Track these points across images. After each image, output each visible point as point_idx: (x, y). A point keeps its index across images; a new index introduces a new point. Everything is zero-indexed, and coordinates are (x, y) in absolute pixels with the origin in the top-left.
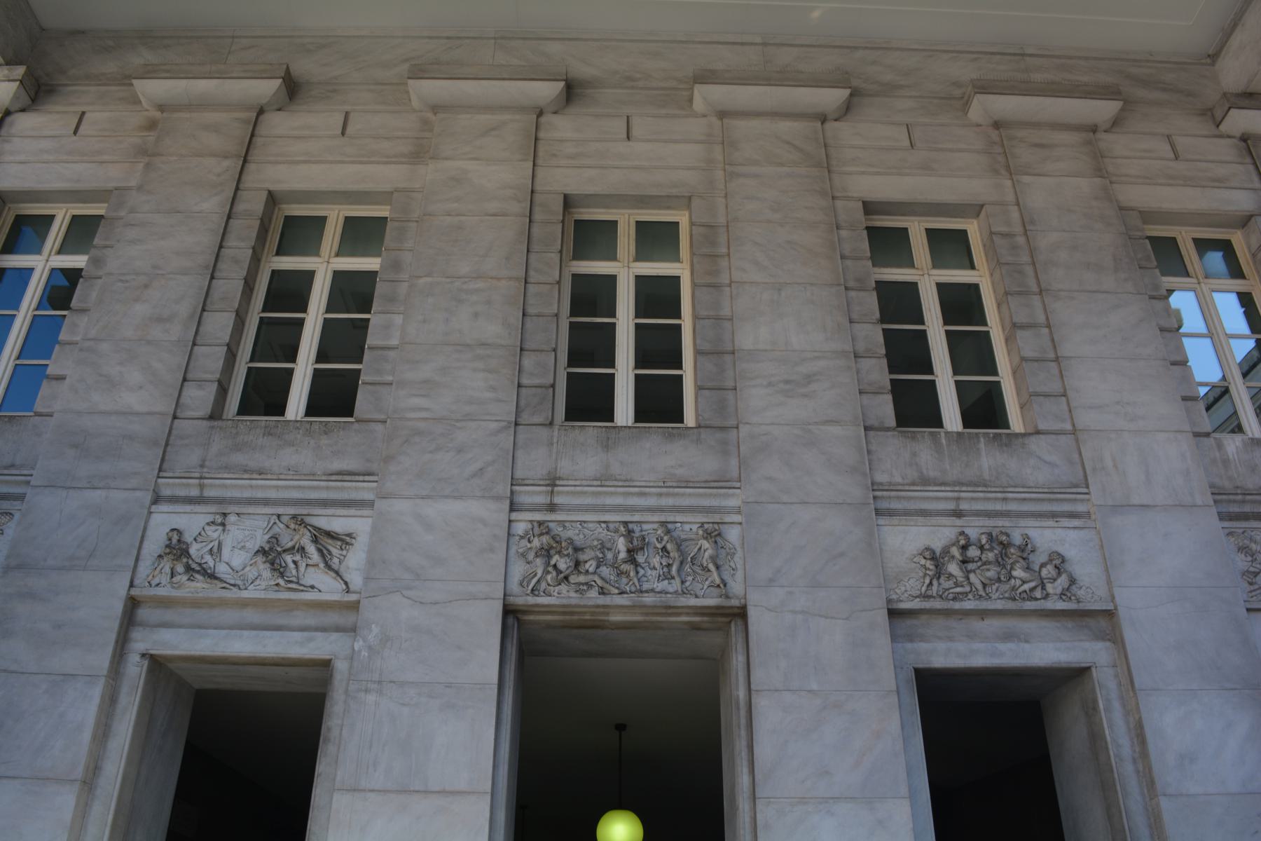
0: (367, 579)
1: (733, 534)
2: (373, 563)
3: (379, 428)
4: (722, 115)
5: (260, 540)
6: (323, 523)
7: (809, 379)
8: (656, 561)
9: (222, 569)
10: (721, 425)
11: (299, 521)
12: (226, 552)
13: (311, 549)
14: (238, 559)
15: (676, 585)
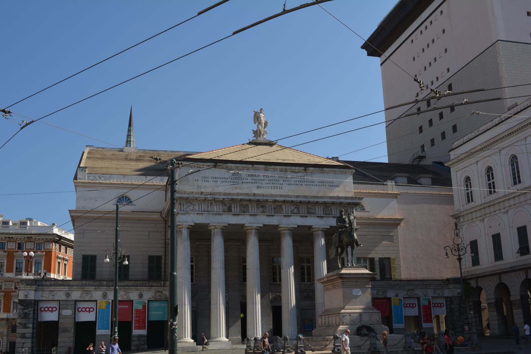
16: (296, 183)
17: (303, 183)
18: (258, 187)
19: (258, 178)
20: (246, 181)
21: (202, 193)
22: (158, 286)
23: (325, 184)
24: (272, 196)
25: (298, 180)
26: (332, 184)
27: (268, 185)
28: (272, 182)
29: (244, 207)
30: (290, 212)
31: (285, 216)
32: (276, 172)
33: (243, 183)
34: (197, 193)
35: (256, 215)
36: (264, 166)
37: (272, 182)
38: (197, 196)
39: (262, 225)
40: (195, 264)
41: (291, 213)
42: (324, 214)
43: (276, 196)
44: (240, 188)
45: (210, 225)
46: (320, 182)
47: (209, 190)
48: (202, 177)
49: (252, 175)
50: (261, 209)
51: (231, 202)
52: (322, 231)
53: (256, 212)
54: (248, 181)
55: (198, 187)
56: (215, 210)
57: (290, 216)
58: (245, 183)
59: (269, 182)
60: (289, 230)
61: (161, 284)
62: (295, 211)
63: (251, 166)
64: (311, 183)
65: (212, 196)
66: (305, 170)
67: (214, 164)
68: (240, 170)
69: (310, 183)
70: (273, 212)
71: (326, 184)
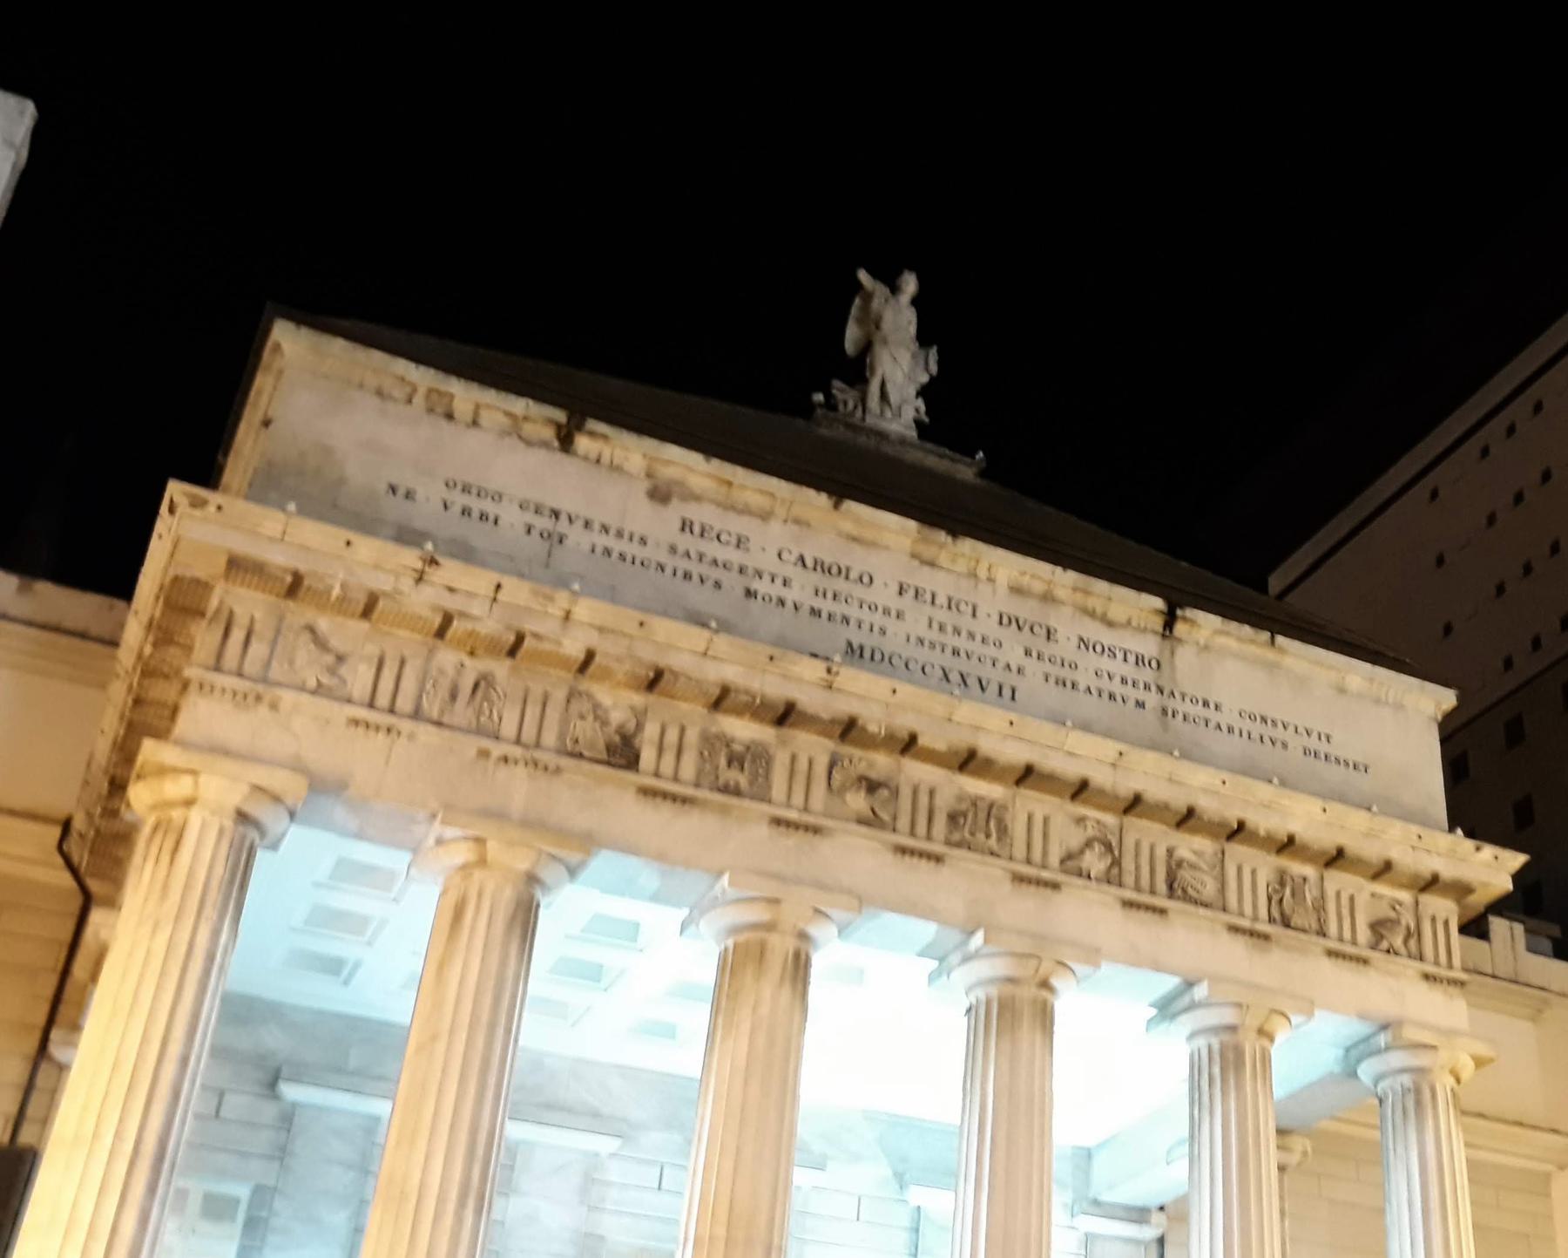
16: (1105, 684)
19: (859, 591)
20: (777, 590)
26: (1323, 748)
27: (923, 655)
29: (735, 760)
32: (985, 588)
33: (750, 594)
37: (951, 641)
49: (819, 565)
50: (858, 801)
51: (638, 699)
54: (790, 595)
56: (509, 728)
58: (767, 599)
59: (934, 635)
64: (1199, 710)
66: (1170, 621)
68: (746, 511)
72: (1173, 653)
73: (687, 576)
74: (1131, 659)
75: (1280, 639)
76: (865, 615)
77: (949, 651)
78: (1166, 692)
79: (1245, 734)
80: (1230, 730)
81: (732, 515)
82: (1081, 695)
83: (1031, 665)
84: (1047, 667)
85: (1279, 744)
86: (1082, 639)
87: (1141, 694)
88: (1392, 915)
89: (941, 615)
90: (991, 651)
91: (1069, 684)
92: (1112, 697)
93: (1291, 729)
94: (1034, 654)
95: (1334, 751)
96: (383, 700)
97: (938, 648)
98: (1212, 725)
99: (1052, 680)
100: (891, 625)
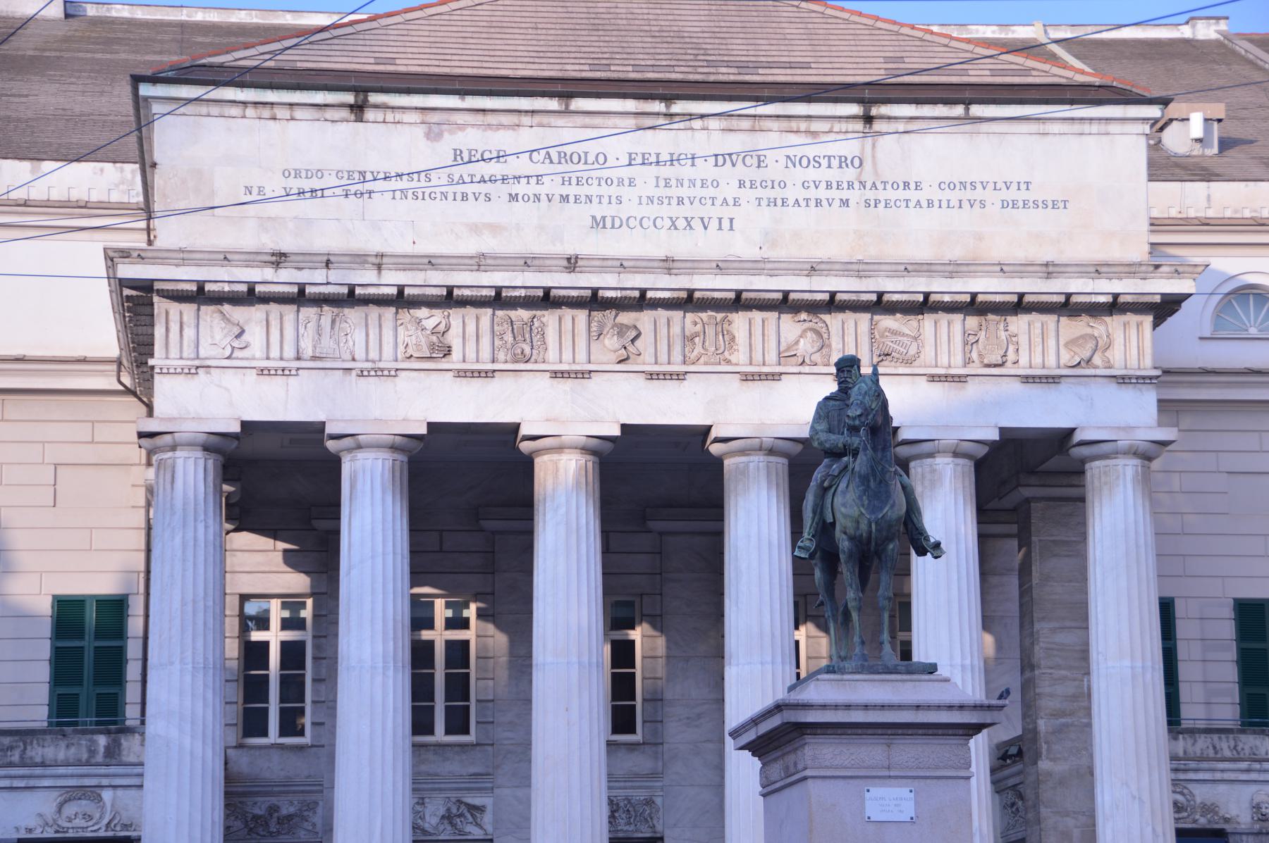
0: (495, 829)
1: (658, 801)
2: (496, 822)
3: (490, 748)
4: (661, 534)
5: (442, 811)
6: (470, 801)
7: (699, 716)
8: (624, 816)
9: (427, 826)
10: (653, 744)
11: (460, 802)
12: (427, 817)
13: (469, 816)
14: (434, 821)
15: (632, 828)
16: (813, 193)
17: (855, 196)
18: (598, 223)
21: (279, 259)
22: (79, 763)
23: (979, 194)
24: (668, 265)
25: (823, 174)
26: (1022, 195)
28: (675, 192)
30: (772, 356)
31: (747, 377)
33: (513, 198)
34: (252, 258)
35: (584, 375)
36: (630, 105)
37: (675, 192)
38: (253, 274)
39: (616, 432)
40: (314, 637)
41: (781, 358)
42: (968, 362)
43: (694, 266)
44: (495, 229)
45: (329, 430)
46: (952, 186)
47: (326, 240)
48: (286, 174)
50: (611, 341)
52: (956, 454)
53: (581, 355)
54: (543, 190)
55: (265, 223)
57: (775, 377)
58: (526, 198)
60: (771, 452)
61: (92, 752)
62: (806, 346)
63: (553, 104)
64: (902, 194)
65: (334, 275)
66: (868, 119)
67: (349, 98)
68: (501, 126)
69: (891, 194)
70: (677, 356)
71: (989, 195)
72: (874, 146)
73: (465, 197)
74: (835, 163)
75: (976, 110)
76: (604, 190)
77: (674, 201)
78: (868, 185)
79: (944, 204)
80: (930, 203)
81: (489, 133)
82: (791, 210)
83: (747, 194)
84: (760, 192)
85: (977, 204)
86: (788, 157)
87: (845, 194)
88: (1089, 331)
89: (665, 171)
90: (711, 192)
91: (779, 202)
92: (818, 203)
93: (991, 186)
94: (748, 184)
95: (1030, 196)
96: (275, 353)
97: (666, 201)
98: (911, 204)
99: (764, 203)
100: (626, 192)
